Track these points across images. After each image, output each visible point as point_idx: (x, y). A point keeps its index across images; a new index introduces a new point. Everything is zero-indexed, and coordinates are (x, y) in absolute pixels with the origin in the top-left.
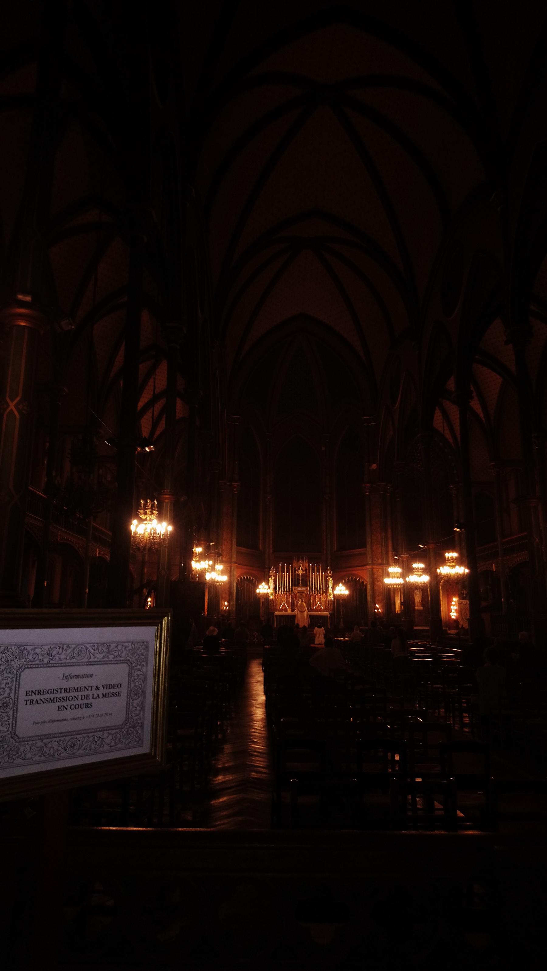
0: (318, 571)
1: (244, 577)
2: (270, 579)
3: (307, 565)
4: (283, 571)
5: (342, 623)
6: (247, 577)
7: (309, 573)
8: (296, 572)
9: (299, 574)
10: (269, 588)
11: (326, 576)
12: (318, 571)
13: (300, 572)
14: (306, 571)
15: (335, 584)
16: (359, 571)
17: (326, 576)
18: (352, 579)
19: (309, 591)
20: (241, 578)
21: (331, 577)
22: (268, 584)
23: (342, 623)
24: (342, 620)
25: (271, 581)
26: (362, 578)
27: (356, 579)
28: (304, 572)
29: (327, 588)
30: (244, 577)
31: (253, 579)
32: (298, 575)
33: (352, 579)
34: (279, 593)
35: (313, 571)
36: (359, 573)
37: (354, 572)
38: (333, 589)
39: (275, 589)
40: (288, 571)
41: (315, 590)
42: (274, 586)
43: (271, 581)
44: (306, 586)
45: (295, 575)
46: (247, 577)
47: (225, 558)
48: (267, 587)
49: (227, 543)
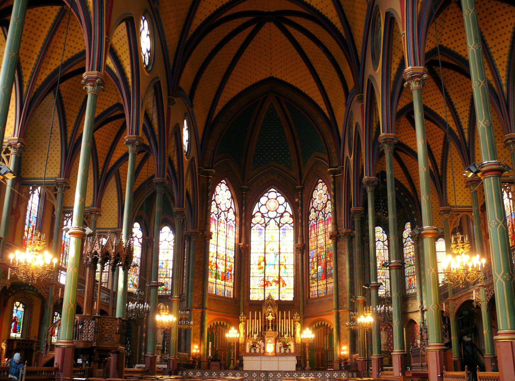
0: (287, 318)
1: (217, 323)
2: (240, 324)
3: (276, 311)
4: (253, 318)
5: (308, 365)
6: (220, 323)
7: (278, 319)
8: (266, 318)
10: (239, 332)
11: (294, 322)
12: (287, 318)
13: (270, 318)
14: (276, 317)
15: (303, 327)
16: (327, 316)
17: (294, 322)
18: (321, 323)
20: (214, 324)
21: (299, 322)
22: (238, 328)
23: (308, 365)
24: (308, 362)
25: (241, 326)
26: (330, 323)
27: (324, 324)
28: (274, 318)
29: (295, 333)
30: (217, 323)
31: (223, 323)
32: (269, 321)
33: (321, 323)
35: (282, 318)
36: (327, 318)
37: (323, 317)
38: (301, 332)
39: (245, 333)
40: (258, 318)
42: (244, 331)
43: (241, 326)
44: (275, 330)
45: (265, 321)
46: (220, 323)
47: (196, 304)
48: (236, 331)
49: (199, 289)
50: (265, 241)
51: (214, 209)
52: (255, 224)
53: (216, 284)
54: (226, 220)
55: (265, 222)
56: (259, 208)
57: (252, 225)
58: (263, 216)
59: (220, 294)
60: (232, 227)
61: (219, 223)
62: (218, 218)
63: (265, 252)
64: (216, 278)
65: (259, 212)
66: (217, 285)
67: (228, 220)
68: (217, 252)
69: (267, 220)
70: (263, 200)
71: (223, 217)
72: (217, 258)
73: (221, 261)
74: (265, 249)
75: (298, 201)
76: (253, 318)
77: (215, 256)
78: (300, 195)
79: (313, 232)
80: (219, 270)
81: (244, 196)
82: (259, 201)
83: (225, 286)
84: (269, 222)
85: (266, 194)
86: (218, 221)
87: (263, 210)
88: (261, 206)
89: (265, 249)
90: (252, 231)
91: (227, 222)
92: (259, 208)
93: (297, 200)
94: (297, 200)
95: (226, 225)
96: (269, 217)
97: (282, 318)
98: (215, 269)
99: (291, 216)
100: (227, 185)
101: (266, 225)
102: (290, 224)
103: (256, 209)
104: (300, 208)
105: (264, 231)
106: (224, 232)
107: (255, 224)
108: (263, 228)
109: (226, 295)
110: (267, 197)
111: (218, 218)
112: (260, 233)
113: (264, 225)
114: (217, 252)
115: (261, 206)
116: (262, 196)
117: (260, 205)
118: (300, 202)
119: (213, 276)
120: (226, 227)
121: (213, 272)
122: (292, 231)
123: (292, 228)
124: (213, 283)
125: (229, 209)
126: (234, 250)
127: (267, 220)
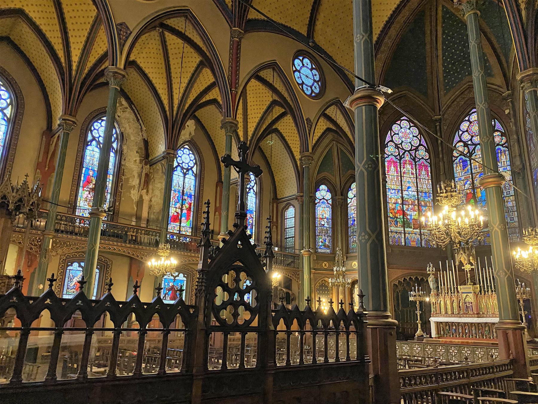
9: (470, 269)
19: (480, 291)
34: (442, 295)
41: (488, 288)
50: (472, 174)
51: (390, 149)
52: (457, 157)
53: (405, 233)
54: (414, 159)
55: (469, 152)
56: (460, 137)
57: (454, 158)
58: (466, 145)
59: (413, 244)
60: (427, 166)
61: (402, 164)
62: (400, 160)
63: (473, 186)
64: (404, 226)
65: (461, 141)
66: (407, 235)
67: (417, 160)
68: (402, 198)
69: (471, 148)
70: (464, 126)
71: (407, 158)
72: (403, 204)
73: (410, 206)
74: (473, 183)
75: (509, 113)
76: (444, 269)
77: (400, 201)
78: (510, 104)
79: (532, 145)
80: (409, 217)
81: (438, 127)
82: (458, 129)
83: (421, 235)
84: (474, 149)
85: (467, 119)
86: (400, 164)
87: (466, 137)
88: (462, 133)
89: (473, 183)
90: (455, 166)
91: (416, 162)
92: (460, 137)
93: (507, 112)
94: (507, 112)
95: (414, 166)
96: (473, 144)
97: (483, 266)
98: (401, 216)
99: (503, 135)
100: (410, 121)
101: (471, 154)
102: (502, 145)
103: (457, 138)
104: (513, 120)
105: (469, 162)
106: (412, 174)
107: (457, 157)
108: (468, 159)
109: (423, 245)
110: (469, 120)
111: (400, 160)
112: (465, 166)
113: (468, 155)
114: (402, 198)
115: (462, 133)
116: (462, 121)
117: (461, 133)
118: (512, 112)
119: (399, 225)
120: (414, 168)
121: (398, 220)
122: (507, 153)
123: (506, 149)
124: (400, 233)
125: (417, 147)
126: (431, 192)
127: (471, 148)
